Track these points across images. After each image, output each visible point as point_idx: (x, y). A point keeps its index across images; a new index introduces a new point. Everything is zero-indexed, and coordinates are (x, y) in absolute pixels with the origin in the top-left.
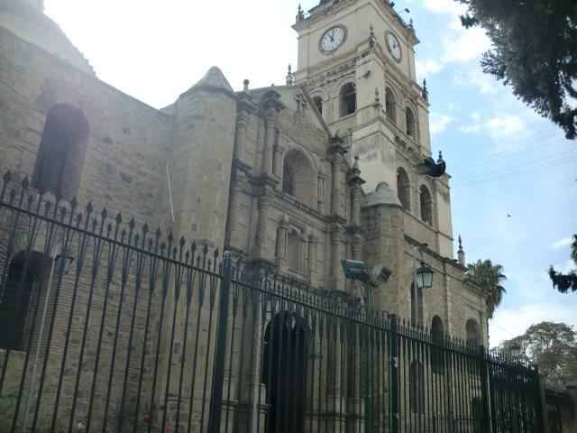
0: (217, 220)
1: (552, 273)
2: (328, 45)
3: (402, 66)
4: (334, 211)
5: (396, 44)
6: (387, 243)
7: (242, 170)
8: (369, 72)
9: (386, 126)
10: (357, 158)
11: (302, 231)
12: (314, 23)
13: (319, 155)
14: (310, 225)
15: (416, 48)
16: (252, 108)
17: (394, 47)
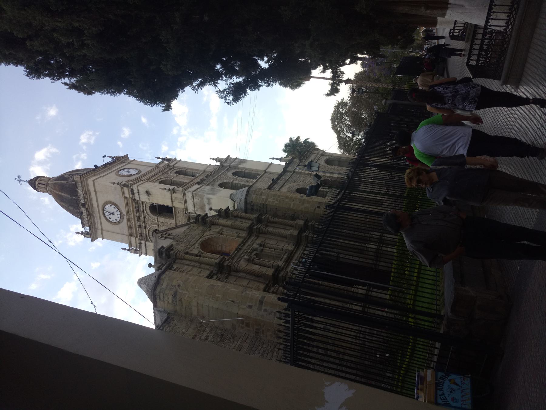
0: (247, 292)
1: (328, 95)
2: (115, 218)
3: (144, 170)
4: (245, 228)
5: (127, 170)
6: (271, 200)
8: (146, 192)
9: (189, 187)
10: (211, 209)
11: (255, 250)
13: (206, 232)
14: (253, 245)
15: (131, 158)
16: (169, 265)
17: (129, 172)
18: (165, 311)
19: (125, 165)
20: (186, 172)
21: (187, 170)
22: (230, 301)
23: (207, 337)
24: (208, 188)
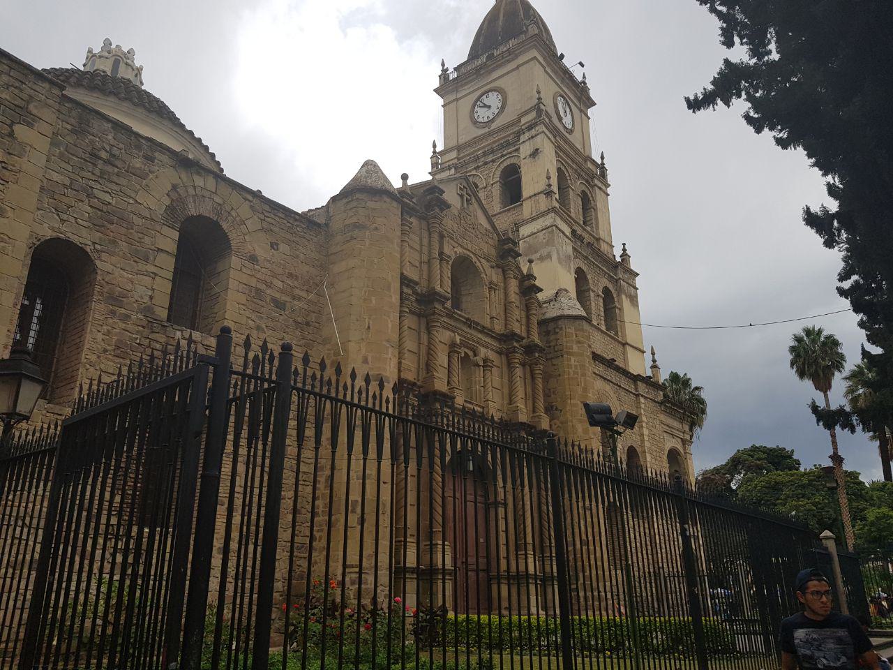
0: (390, 350)
2: (483, 115)
3: (575, 139)
7: (408, 286)
8: (537, 150)
9: (562, 219)
10: (531, 261)
11: (474, 352)
12: (462, 86)
13: (488, 261)
15: (590, 112)
16: (413, 209)
18: (329, 218)
19: (576, 106)
20: (590, 209)
21: (592, 210)
22: (369, 324)
23: (300, 299)
24: (569, 249)
